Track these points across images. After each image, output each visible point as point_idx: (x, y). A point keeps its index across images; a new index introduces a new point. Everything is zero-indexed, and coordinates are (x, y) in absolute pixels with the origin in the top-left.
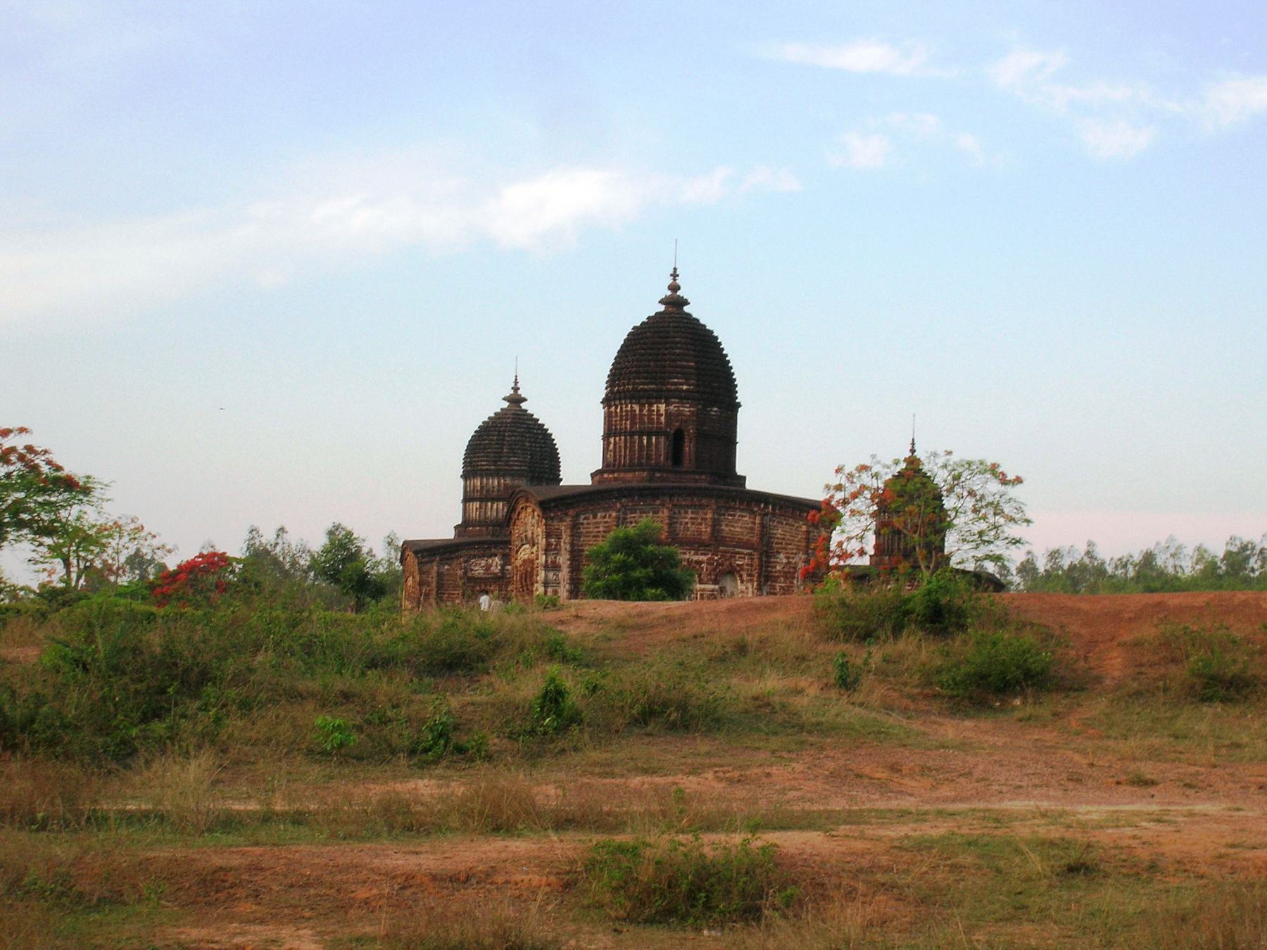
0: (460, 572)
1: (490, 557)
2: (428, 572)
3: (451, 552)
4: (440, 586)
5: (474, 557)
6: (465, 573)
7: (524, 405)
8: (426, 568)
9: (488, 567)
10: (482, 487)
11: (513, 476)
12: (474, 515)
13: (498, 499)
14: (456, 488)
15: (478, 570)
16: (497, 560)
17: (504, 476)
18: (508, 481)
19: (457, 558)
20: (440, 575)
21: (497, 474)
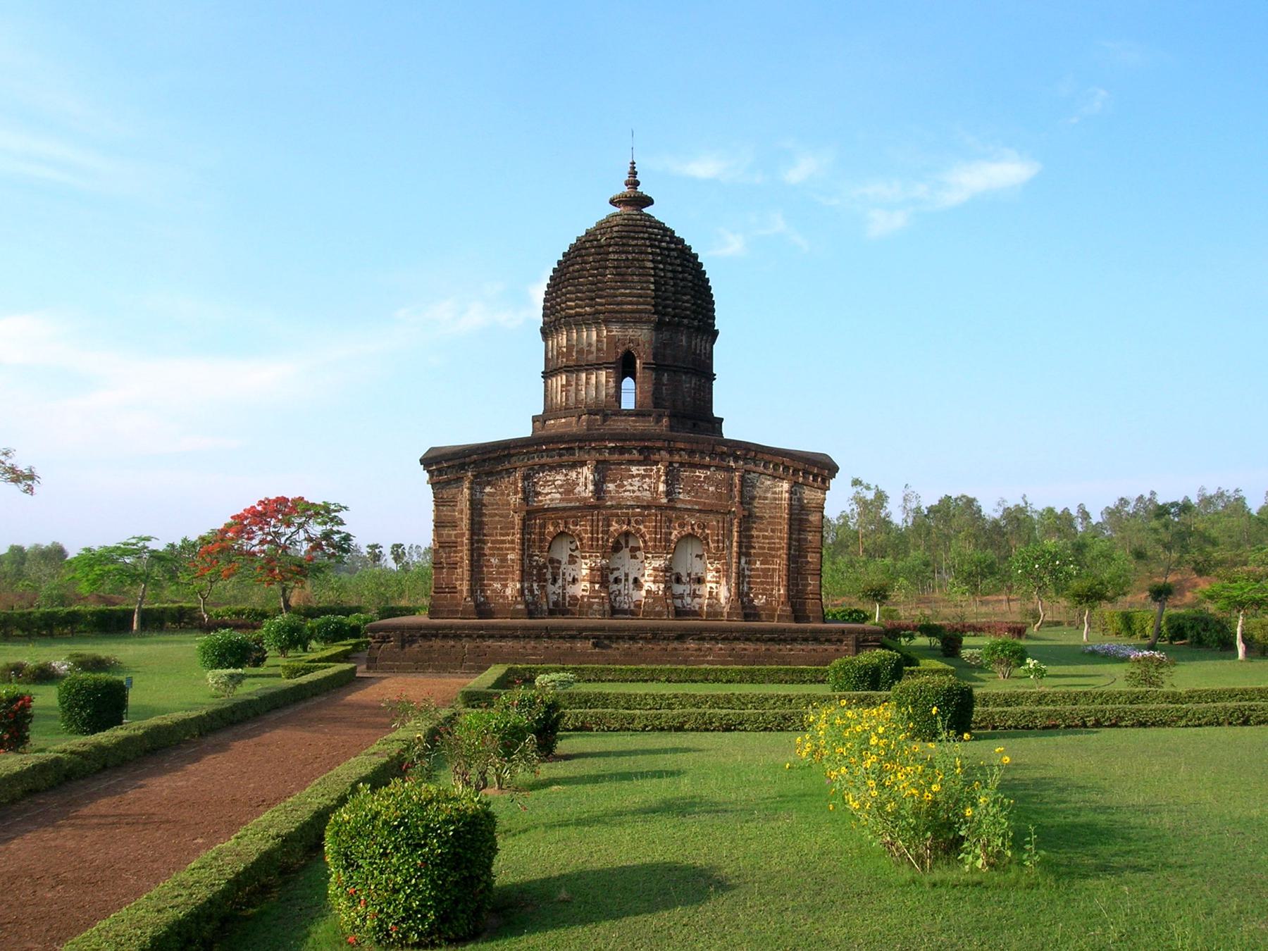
0: (515, 499)
1: (574, 465)
2: (452, 502)
3: (499, 460)
4: (477, 527)
5: (542, 467)
6: (525, 499)
7: (639, 189)
8: (446, 493)
9: (569, 488)
10: (570, 347)
11: (623, 322)
12: (559, 398)
13: (597, 366)
14: (535, 353)
15: (550, 492)
16: (587, 472)
17: (607, 322)
18: (616, 331)
19: (509, 472)
20: (476, 507)
21: (594, 320)
